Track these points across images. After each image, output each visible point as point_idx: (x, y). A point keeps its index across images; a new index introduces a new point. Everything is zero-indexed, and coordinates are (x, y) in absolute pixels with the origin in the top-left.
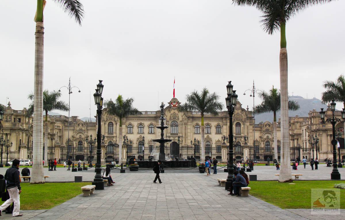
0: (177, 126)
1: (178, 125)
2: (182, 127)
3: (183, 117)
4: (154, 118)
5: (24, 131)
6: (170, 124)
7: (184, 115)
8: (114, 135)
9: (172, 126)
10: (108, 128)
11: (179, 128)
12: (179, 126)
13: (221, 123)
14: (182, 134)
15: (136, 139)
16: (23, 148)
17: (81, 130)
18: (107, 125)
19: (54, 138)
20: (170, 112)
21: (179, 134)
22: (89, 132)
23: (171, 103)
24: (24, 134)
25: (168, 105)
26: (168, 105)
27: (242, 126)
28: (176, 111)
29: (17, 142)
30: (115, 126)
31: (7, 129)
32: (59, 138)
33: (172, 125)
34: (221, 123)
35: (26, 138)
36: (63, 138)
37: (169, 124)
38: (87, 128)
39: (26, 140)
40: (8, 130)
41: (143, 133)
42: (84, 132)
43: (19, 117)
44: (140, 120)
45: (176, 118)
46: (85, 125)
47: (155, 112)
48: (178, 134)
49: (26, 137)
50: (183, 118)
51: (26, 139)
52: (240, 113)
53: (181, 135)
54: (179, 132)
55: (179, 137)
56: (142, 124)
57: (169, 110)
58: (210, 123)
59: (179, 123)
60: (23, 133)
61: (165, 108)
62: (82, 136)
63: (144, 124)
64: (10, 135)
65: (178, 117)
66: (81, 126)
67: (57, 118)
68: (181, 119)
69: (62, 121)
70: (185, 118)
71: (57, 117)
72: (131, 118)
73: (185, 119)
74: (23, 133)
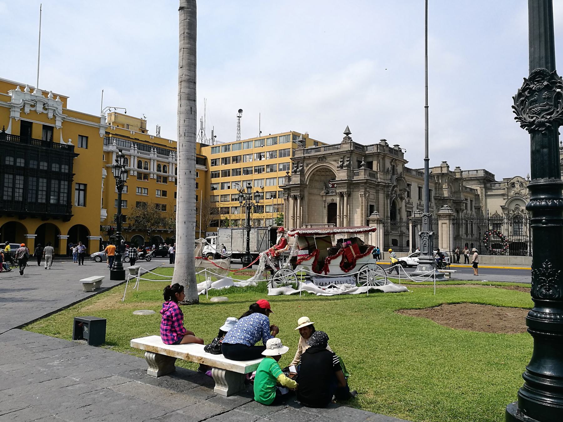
24: (381, 196)
29: (362, 211)
31: (341, 184)
39: (387, 208)
43: (370, 160)
51: (387, 205)
60: (377, 192)
64: (349, 195)
74: (377, 192)
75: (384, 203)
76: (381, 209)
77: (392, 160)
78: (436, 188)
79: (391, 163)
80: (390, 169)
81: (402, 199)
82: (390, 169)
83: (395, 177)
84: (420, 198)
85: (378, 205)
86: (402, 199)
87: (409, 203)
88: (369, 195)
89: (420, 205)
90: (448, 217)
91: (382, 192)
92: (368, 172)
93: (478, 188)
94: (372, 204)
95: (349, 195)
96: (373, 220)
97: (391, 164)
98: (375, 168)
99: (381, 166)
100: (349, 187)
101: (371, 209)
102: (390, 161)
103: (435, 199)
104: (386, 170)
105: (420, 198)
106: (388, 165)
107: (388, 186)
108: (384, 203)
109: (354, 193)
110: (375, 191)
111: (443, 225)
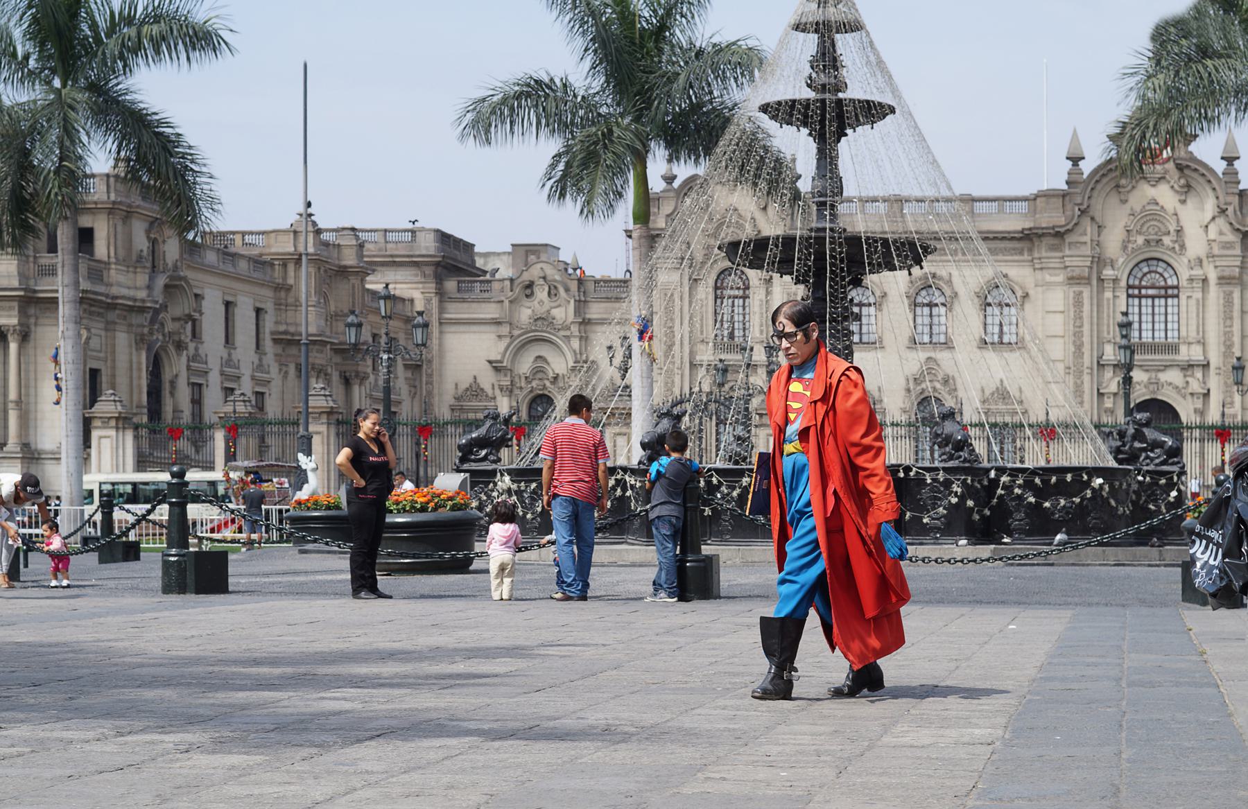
0: (1173, 296)
1: (1177, 287)
2: (1202, 304)
3: (1212, 234)
4: (1020, 239)
5: (112, 316)
6: (1123, 283)
7: (1221, 221)
9: (1140, 297)
11: (1183, 309)
12: (1183, 297)
14: (1203, 343)
15: (903, 382)
16: (105, 425)
17: (543, 320)
18: (711, 290)
19: (357, 374)
20: (1124, 202)
21: (1183, 349)
22: (592, 336)
24: (122, 339)
32: (409, 375)
33: (1140, 288)
35: (139, 363)
36: (430, 376)
37: (1116, 281)
38: (578, 312)
40: (11, 308)
41: (948, 345)
42: (562, 333)
45: (1167, 240)
46: (567, 290)
47: (1025, 199)
48: (1174, 348)
49: (139, 356)
50: (1212, 235)
51: (140, 369)
53: (1196, 354)
54: (1183, 333)
55: (1188, 367)
56: (941, 278)
57: (1118, 186)
59: (1184, 274)
61: (1095, 171)
62: (550, 359)
63: (950, 282)
65: (1179, 232)
66: (541, 293)
67: (389, 246)
68: (1196, 244)
69: (427, 264)
70: (1224, 238)
71: (390, 236)
73: (1227, 246)
75: (131, 362)
76: (122, 380)
77: (152, 223)
78: (278, 304)
79: (148, 232)
80: (145, 253)
81: (180, 346)
82: (145, 253)
83: (161, 281)
84: (229, 339)
85: (114, 368)
86: (180, 346)
87: (195, 358)
88: (88, 339)
89: (229, 362)
90: (325, 416)
91: (125, 328)
92: (83, 269)
94: (95, 365)
95: (25, 337)
96: (106, 421)
97: (148, 237)
98: (101, 248)
99: (119, 243)
100: (23, 313)
101: (93, 385)
102: (146, 225)
103: (275, 341)
104: (134, 258)
105: (229, 339)
106: (141, 243)
107: (142, 310)
108: (131, 362)
109: (39, 329)
110: (102, 325)
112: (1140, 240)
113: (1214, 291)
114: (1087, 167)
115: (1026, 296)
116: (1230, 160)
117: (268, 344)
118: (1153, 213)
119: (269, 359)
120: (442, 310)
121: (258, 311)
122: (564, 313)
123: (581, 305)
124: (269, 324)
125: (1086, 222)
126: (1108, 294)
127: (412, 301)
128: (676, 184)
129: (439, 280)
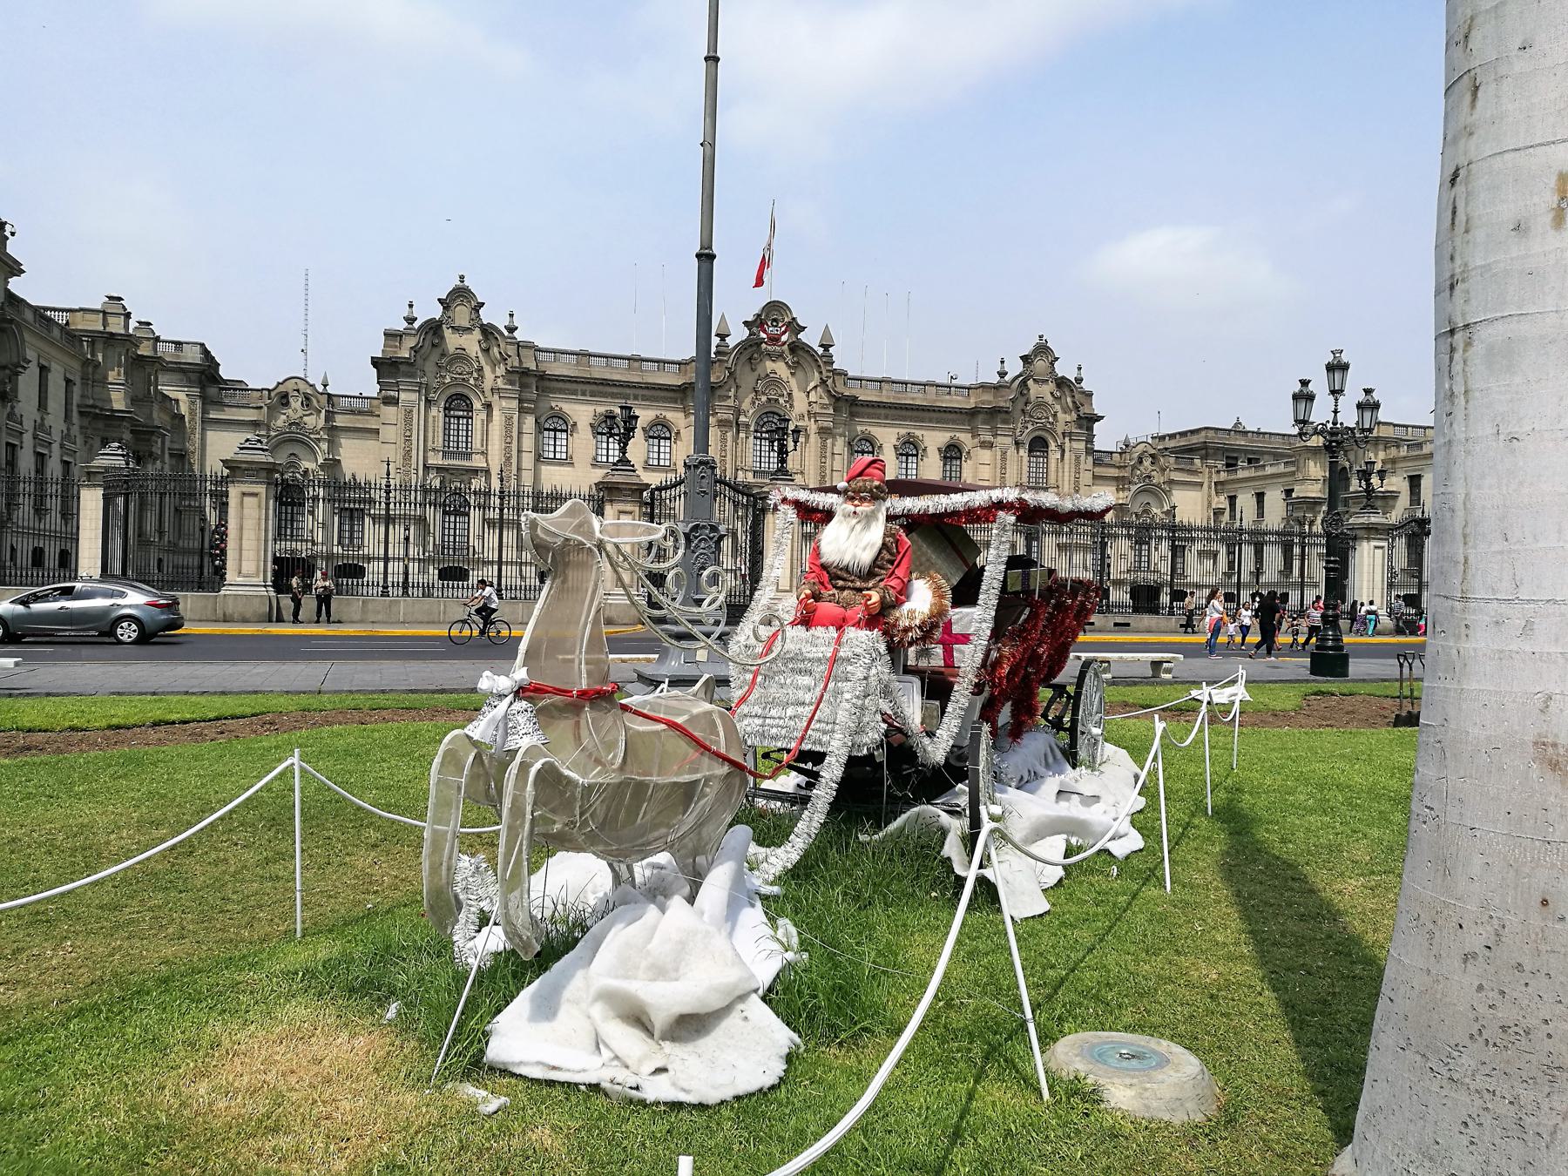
3: (813, 397)
8: (478, 462)
10: (447, 429)
13: (965, 438)
19: (151, 454)
20: (753, 370)
23: (755, 324)
25: (744, 333)
26: (744, 333)
27: (1054, 455)
28: (781, 369)
30: (479, 417)
34: (965, 438)
37: (748, 426)
44: (605, 395)
52: (1050, 399)
58: (918, 433)
68: (800, 404)
72: (561, 385)
73: (823, 406)
90: (264, 474)
93: (182, 396)
103: (81, 413)
111: (246, 499)
112: (764, 399)
113: (813, 438)
114: (732, 342)
115: (678, 433)
116: (826, 347)
117: (75, 414)
118: (774, 382)
119: (75, 430)
120: (204, 412)
121: (68, 381)
122: (315, 421)
123: (330, 416)
124: (76, 399)
125: (731, 382)
126: (742, 435)
127: (177, 401)
128: (416, 325)
129: (203, 388)
